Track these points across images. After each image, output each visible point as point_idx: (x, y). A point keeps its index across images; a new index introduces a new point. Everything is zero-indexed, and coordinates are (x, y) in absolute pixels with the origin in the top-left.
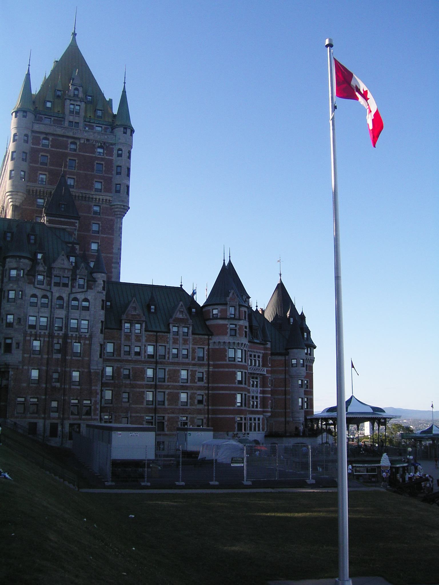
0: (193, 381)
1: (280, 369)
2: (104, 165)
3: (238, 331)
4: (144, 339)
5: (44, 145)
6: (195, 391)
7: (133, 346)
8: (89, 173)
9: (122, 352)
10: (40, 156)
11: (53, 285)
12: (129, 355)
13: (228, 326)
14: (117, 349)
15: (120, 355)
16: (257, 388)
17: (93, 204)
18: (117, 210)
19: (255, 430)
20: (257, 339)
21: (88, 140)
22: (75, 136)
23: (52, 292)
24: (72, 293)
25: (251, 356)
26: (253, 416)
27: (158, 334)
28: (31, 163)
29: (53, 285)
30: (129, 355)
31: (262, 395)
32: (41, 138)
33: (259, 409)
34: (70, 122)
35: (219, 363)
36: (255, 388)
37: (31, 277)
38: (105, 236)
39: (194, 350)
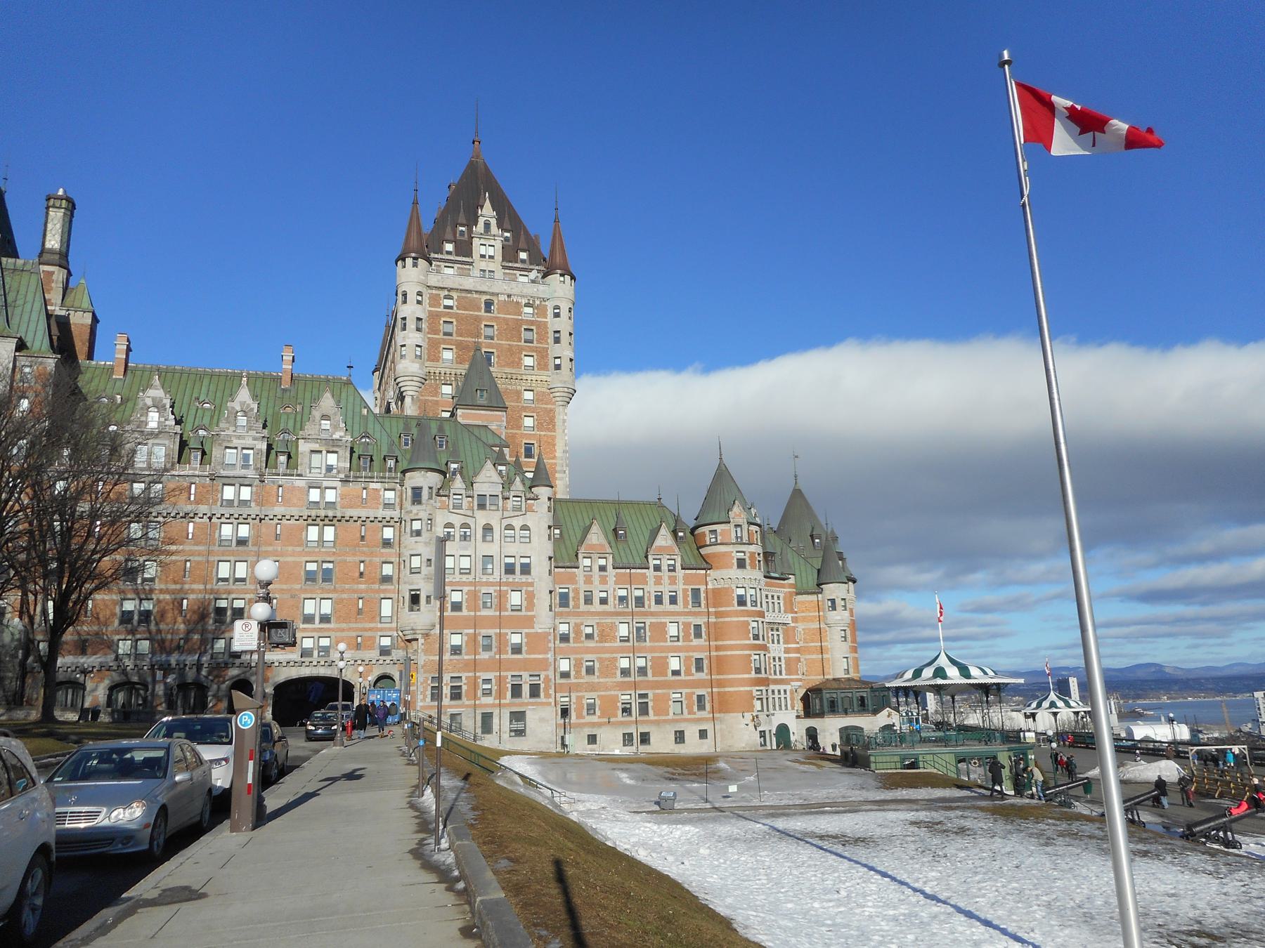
0: (687, 638)
1: (811, 614)
2: (535, 331)
3: (748, 561)
4: (611, 580)
5: (446, 307)
6: (691, 654)
8: (515, 343)
10: (442, 322)
12: (592, 604)
13: (733, 554)
15: (577, 606)
18: (558, 394)
19: (781, 709)
21: (509, 296)
22: (490, 291)
25: (767, 596)
27: (633, 571)
28: (428, 333)
29: (476, 507)
32: (442, 296)
33: (784, 676)
34: (481, 270)
35: (723, 609)
37: (444, 498)
39: (685, 591)
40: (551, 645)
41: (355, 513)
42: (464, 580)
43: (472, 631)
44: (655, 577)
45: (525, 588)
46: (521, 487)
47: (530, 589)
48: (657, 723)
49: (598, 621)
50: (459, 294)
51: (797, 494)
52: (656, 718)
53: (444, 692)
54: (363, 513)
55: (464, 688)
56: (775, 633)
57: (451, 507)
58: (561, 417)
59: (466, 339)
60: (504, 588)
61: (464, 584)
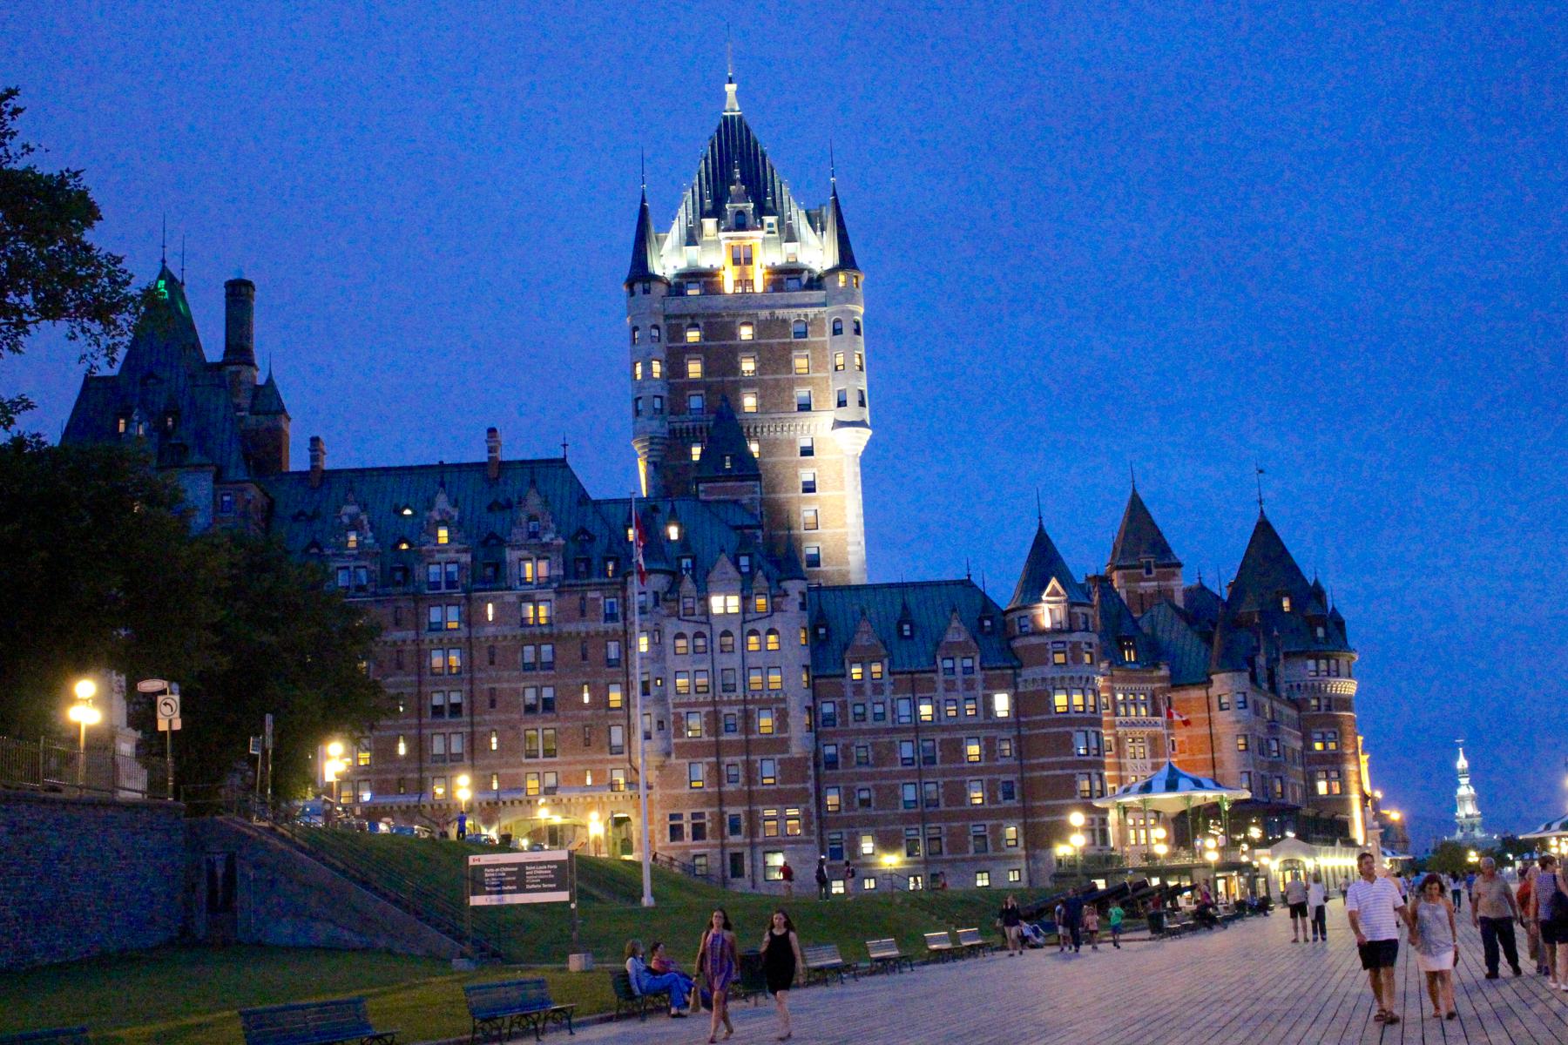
4: (888, 690)
6: (996, 776)
7: (869, 705)
9: (851, 717)
13: (1049, 647)
15: (848, 725)
27: (916, 676)
30: (864, 720)
37: (672, 604)
40: (811, 772)
41: (570, 628)
42: (701, 699)
43: (713, 759)
44: (946, 681)
45: (775, 706)
46: (766, 584)
47: (782, 706)
48: (952, 862)
51: (1264, 529)
52: (950, 857)
53: (685, 830)
54: (582, 627)
55: (709, 825)
60: (751, 707)
61: (704, 704)
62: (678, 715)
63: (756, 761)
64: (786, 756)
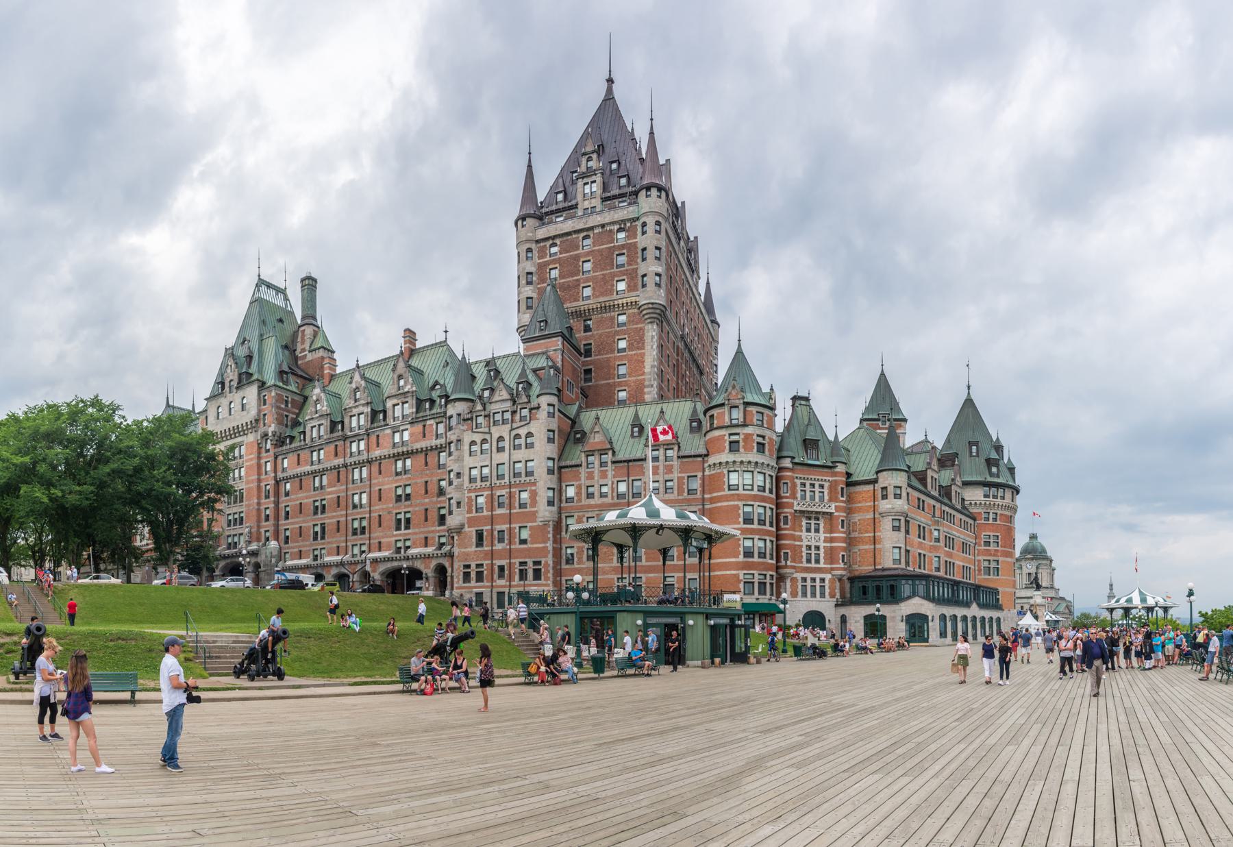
11: (492, 424)
14: (578, 493)
15: (580, 500)
16: (817, 534)
17: (617, 313)
18: (645, 312)
19: (814, 595)
20: (818, 460)
23: (491, 433)
24: (512, 429)
26: (809, 576)
29: (492, 424)
31: (828, 545)
32: (548, 246)
33: (822, 565)
36: (812, 534)
37: (470, 422)
38: (634, 352)
40: (550, 535)
47: (533, 488)
49: (597, 513)
50: (561, 239)
56: (813, 522)
57: (474, 427)
58: (650, 334)
59: (568, 279)
60: (513, 490)
62: (469, 498)
63: (515, 528)
64: (534, 524)
